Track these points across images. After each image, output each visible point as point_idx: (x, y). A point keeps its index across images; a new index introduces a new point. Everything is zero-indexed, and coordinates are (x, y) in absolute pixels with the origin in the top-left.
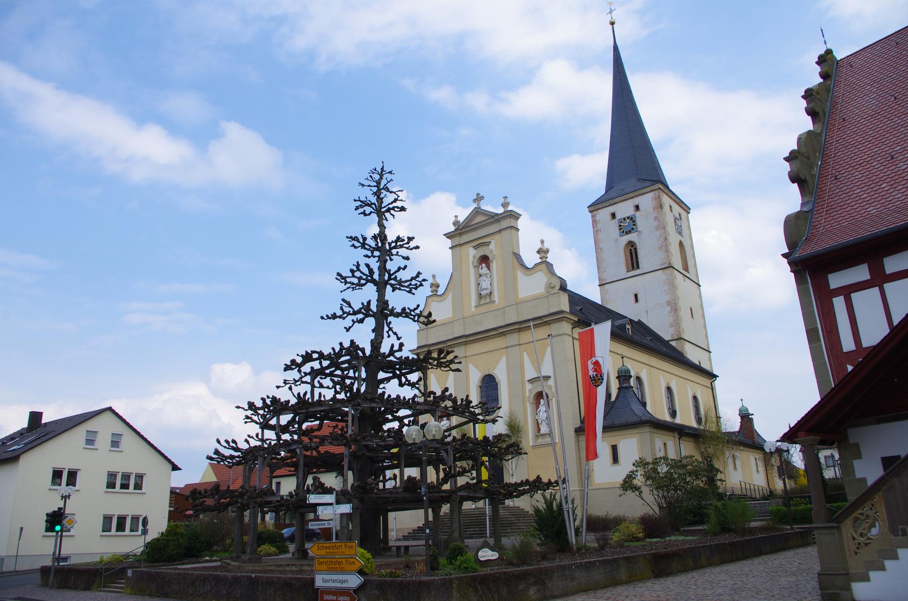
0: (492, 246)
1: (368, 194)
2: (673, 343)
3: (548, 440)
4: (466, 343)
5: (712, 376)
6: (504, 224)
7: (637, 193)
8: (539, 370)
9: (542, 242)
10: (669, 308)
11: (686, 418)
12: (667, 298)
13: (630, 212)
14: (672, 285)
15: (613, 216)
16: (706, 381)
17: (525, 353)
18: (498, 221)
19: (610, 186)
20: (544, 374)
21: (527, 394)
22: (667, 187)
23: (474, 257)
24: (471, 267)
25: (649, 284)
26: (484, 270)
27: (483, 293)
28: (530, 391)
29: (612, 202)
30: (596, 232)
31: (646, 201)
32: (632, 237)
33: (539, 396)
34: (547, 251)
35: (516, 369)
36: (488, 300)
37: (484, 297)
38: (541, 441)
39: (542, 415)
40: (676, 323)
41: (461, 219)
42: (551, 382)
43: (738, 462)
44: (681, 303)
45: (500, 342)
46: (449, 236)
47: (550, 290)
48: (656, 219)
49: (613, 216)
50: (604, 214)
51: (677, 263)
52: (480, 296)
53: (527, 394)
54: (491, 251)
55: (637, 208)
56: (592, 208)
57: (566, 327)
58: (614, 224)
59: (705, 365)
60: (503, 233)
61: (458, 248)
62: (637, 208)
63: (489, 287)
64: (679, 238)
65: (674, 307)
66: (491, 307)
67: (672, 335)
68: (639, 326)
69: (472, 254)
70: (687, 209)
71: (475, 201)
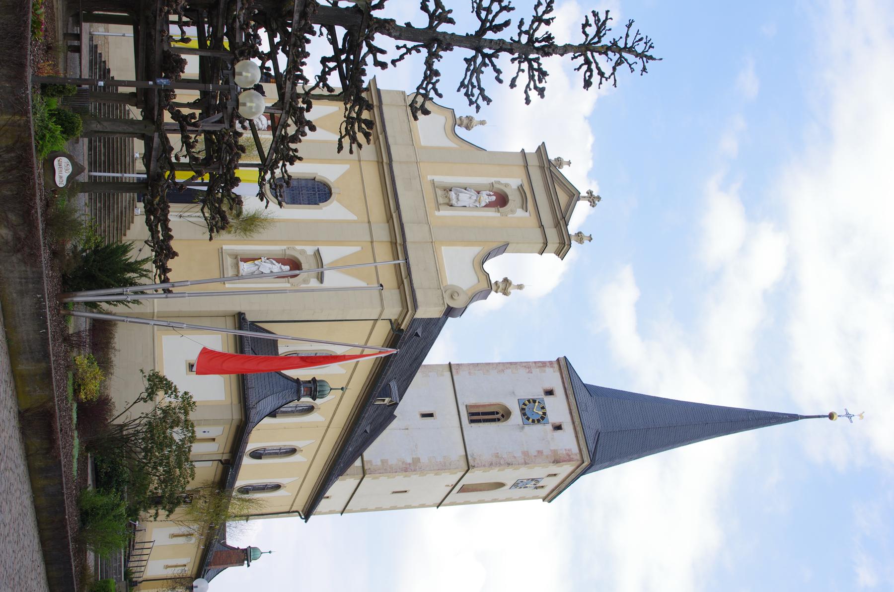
0: (520, 213)
2: (358, 463)
3: (230, 272)
4: (380, 163)
5: (307, 514)
7: (579, 429)
8: (333, 267)
9: (520, 287)
10: (409, 461)
11: (249, 472)
12: (424, 460)
14: (442, 467)
15: (550, 393)
16: (300, 504)
17: (358, 248)
18: (557, 225)
19: (592, 390)
20: (327, 274)
21: (299, 247)
22: (584, 473)
23: (506, 185)
24: (493, 180)
25: (446, 435)
26: (485, 199)
27: (452, 194)
28: (303, 252)
29: (570, 392)
30: (528, 366)
31: (567, 441)
32: (516, 417)
33: (295, 265)
34: (505, 293)
35: (336, 233)
36: (441, 200)
37: (446, 195)
38: (229, 261)
39: (267, 267)
40: (386, 469)
41: (565, 171)
42: (314, 283)
43: (182, 540)
44: (415, 477)
45: (378, 212)
46: (541, 150)
47: (448, 292)
48: (540, 452)
49: (550, 393)
50: (554, 380)
51: (472, 478)
52: (448, 189)
53: (299, 247)
54: (513, 212)
55: (558, 427)
56: (563, 363)
57: (393, 311)
58: (538, 394)
59: (323, 504)
61: (521, 162)
62: (558, 427)
63: (461, 204)
64: (510, 483)
65: (411, 468)
66: (430, 204)
67: (370, 462)
68: (387, 416)
69: (512, 182)
70: (549, 498)
71: (590, 193)
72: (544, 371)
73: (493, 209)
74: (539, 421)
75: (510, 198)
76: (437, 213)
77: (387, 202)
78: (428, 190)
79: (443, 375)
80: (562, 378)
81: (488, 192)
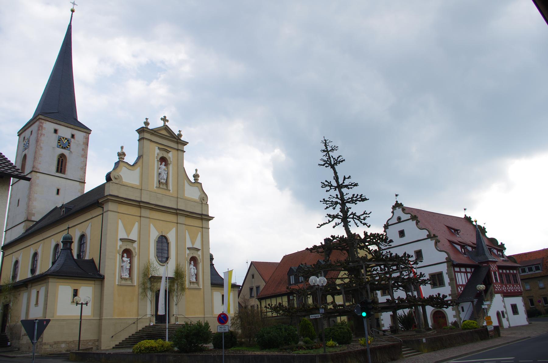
1: (324, 148)
6: (180, 147)
8: (193, 243)
13: (69, 137)
15: (56, 131)
23: (158, 154)
26: (163, 167)
45: (173, 218)
48: (83, 150)
49: (56, 131)
54: (170, 158)
55: (73, 136)
58: (55, 137)
61: (149, 142)
62: (73, 136)
71: (162, 119)
72: (45, 128)
74: (69, 143)
76: (171, 191)
78: (160, 191)
79: (39, 177)
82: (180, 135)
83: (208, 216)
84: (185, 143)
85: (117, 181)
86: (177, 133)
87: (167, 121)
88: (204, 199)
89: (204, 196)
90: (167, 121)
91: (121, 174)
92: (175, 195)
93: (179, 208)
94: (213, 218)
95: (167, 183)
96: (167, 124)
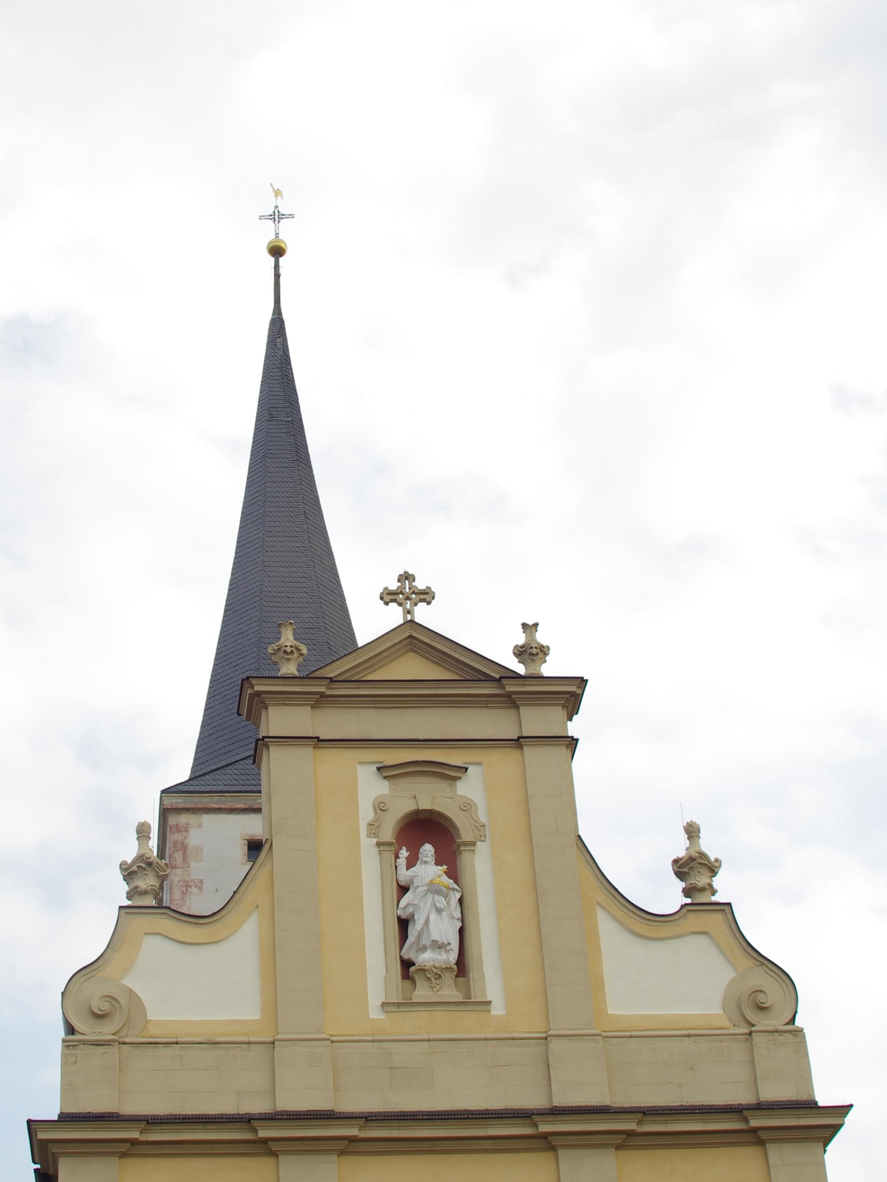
0: (471, 787)
6: (536, 720)
9: (692, 831)
23: (380, 807)
24: (367, 844)
26: (428, 870)
54: (468, 807)
56: (178, 801)
60: (531, 753)
61: (305, 753)
66: (467, 1023)
72: (199, 850)
73: (465, 857)
75: (425, 805)
76: (498, 1009)
77: (487, 1144)
78: (413, 1023)
80: (219, 810)
81: (402, 862)
82: (532, 652)
83: (811, 1106)
84: (569, 694)
85: (105, 1031)
86: (500, 650)
87: (426, 596)
88: (765, 1000)
89: (761, 979)
90: (426, 596)
91: (129, 982)
92: (536, 1028)
93: (561, 1100)
94: (844, 1110)
95: (461, 967)
96: (423, 614)
